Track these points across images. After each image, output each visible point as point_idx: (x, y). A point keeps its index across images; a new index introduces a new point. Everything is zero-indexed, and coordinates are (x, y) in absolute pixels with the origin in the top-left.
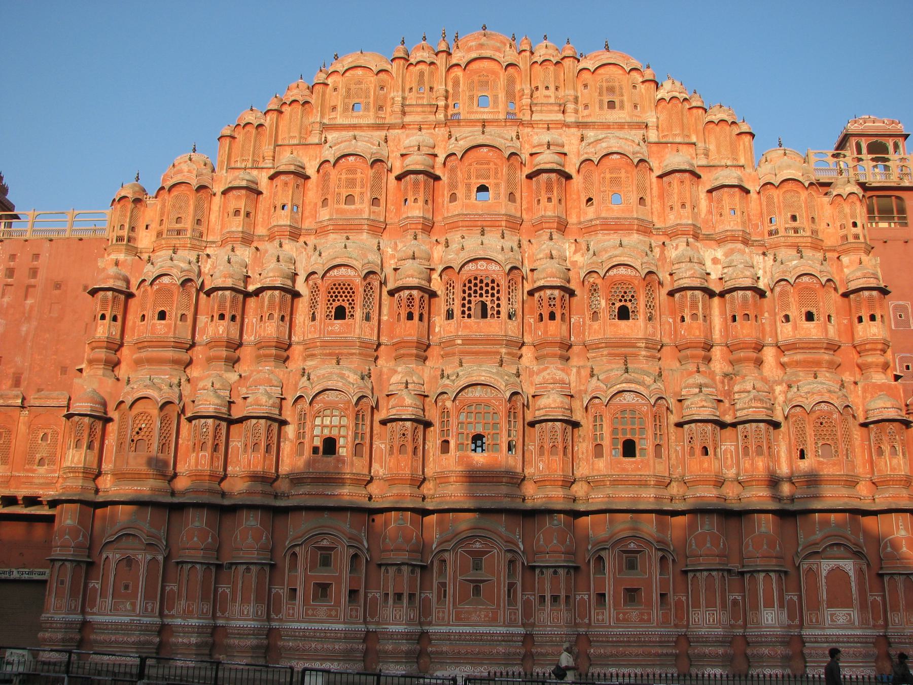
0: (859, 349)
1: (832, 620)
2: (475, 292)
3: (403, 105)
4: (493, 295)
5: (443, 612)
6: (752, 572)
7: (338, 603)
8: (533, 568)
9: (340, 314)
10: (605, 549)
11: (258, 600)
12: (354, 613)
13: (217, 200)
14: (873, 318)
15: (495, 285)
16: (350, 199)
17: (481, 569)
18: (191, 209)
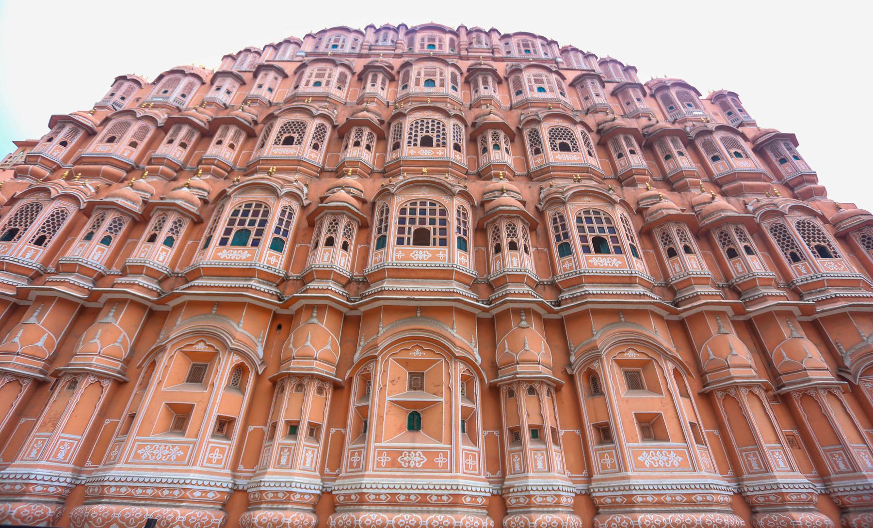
2: (422, 129)
4: (438, 132)
5: (360, 455)
9: (289, 141)
16: (318, 84)
17: (422, 388)
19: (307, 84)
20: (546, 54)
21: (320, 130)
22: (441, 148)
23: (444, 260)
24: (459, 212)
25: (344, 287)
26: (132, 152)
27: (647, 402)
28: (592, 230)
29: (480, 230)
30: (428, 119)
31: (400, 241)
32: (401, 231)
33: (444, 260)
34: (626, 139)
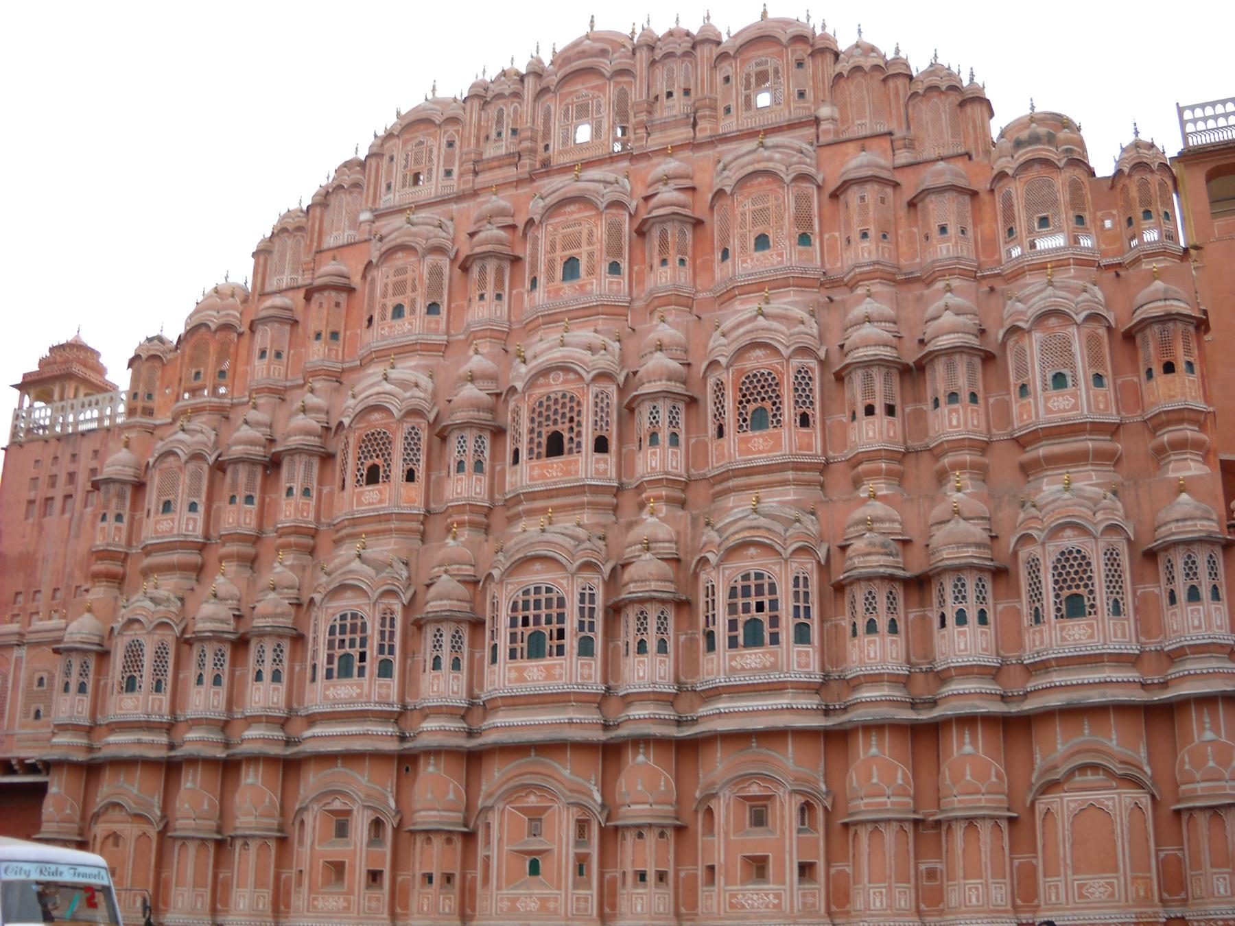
0: (1156, 424)
1: (1081, 896)
3: (475, 162)
4: (571, 420)
6: (949, 821)
7: (351, 892)
8: (616, 828)
9: (373, 476)
10: (714, 796)
11: (259, 883)
12: (374, 904)
13: (245, 340)
14: (1169, 368)
15: (574, 404)
16: (398, 311)
18: (212, 359)
19: (383, 318)
20: (802, 94)
21: (412, 440)
22: (575, 456)
23: (561, 675)
24: (582, 595)
25: (463, 718)
26: (195, 520)
27: (757, 841)
28: (746, 609)
29: (614, 611)
30: (555, 392)
31: (513, 655)
32: (513, 638)
33: (561, 675)
34: (868, 377)
